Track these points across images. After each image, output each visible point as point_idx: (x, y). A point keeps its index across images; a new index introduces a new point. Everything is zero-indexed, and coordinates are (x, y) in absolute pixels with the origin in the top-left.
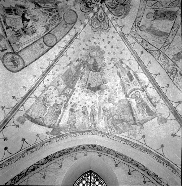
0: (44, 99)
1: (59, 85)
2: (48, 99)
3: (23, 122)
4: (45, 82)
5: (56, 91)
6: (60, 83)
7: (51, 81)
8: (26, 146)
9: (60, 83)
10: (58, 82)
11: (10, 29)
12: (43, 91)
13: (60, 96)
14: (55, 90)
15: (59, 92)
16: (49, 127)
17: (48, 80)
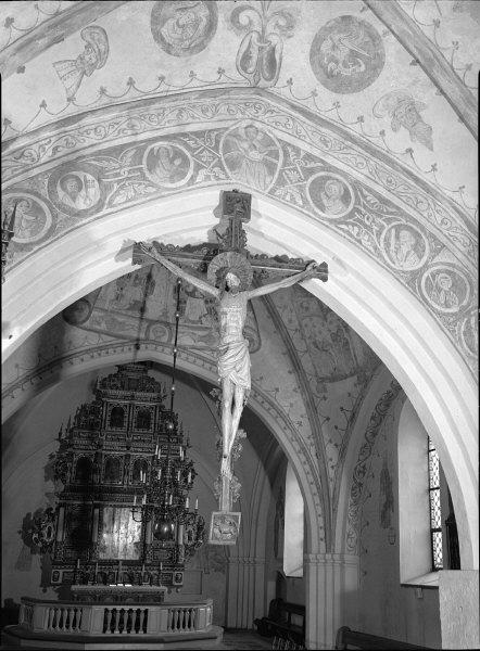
0: (315, 343)
1: (307, 309)
2: (319, 338)
3: (325, 390)
4: (291, 327)
5: (315, 319)
6: (305, 305)
7: (294, 319)
8: (349, 415)
9: (305, 305)
10: (301, 306)
11: (203, 319)
12: (303, 337)
13: (326, 319)
14: (311, 320)
15: (319, 316)
16: (352, 375)
17: (290, 321)
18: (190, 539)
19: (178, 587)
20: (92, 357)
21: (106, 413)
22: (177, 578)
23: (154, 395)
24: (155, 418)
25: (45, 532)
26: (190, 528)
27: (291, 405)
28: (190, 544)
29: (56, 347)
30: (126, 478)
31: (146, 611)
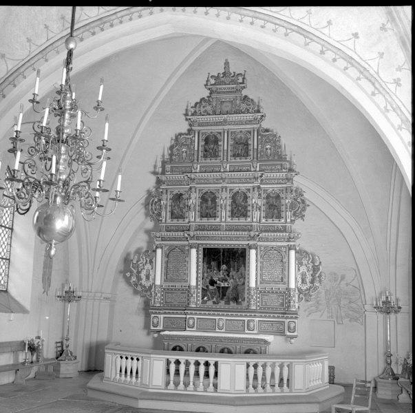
18: (303, 281)
19: (292, 337)
20: (94, 34)
21: (198, 144)
22: (289, 328)
23: (249, 116)
24: (254, 143)
25: (143, 275)
26: (303, 269)
27: (381, 55)
28: (304, 288)
29: (46, 27)
30: (224, 214)
31: (216, 365)
